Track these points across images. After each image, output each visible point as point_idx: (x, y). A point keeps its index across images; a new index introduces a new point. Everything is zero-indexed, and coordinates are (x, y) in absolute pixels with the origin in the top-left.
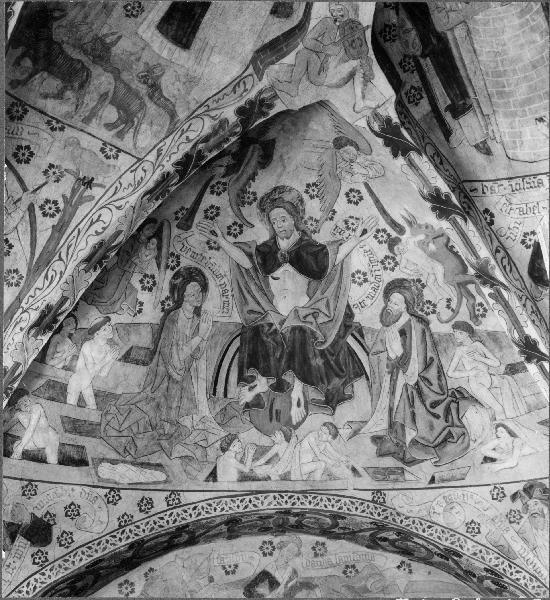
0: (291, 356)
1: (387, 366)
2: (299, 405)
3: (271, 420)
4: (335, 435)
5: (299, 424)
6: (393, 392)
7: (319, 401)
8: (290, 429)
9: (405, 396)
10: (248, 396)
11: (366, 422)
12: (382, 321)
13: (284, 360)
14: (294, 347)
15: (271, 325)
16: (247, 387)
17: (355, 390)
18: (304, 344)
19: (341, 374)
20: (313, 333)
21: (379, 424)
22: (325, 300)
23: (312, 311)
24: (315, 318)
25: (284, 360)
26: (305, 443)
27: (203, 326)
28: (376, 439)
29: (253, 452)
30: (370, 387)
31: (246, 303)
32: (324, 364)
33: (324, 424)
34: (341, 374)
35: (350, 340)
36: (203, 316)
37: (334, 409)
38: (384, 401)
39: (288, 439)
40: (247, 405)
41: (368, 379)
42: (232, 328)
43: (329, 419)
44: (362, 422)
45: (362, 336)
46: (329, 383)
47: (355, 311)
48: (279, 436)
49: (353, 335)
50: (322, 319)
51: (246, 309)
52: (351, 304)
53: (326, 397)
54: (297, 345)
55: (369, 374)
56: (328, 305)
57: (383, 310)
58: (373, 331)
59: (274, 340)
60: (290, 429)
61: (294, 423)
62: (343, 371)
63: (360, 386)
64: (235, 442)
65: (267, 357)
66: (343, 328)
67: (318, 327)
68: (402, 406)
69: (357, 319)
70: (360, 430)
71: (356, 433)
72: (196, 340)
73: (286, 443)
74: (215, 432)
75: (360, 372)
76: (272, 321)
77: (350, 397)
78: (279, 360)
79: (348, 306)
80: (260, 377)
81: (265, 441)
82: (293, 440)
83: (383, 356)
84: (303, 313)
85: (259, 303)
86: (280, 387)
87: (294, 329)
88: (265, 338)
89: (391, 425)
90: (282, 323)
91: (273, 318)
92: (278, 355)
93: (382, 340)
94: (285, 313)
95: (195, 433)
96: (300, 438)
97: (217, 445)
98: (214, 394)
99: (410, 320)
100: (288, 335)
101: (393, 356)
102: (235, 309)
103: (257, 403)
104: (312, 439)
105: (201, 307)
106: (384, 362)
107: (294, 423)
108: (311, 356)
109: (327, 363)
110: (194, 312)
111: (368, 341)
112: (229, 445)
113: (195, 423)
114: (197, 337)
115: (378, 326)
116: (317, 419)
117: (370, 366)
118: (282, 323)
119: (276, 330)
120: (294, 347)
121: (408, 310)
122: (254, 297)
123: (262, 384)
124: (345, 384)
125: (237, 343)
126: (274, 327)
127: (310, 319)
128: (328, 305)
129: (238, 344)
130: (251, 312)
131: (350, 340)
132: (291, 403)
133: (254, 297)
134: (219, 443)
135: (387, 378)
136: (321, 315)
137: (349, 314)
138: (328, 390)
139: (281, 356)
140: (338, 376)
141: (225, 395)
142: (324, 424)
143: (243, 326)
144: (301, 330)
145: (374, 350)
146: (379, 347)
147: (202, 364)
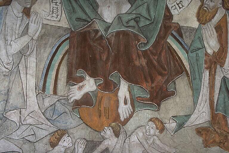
0: (116, 59)
1: (206, 62)
2: (126, 103)
3: (100, 116)
4: (162, 129)
5: (127, 120)
6: (212, 86)
7: (143, 99)
8: (119, 126)
9: (224, 89)
10: (77, 94)
11: (190, 115)
12: (199, 20)
13: (109, 63)
14: (118, 51)
15: (97, 31)
16: (76, 87)
17: (177, 87)
18: (127, 46)
19: (164, 72)
20: (136, 36)
21: (201, 115)
22: (146, 5)
23: (134, 16)
24: (137, 22)
25: (109, 63)
26: (134, 138)
27: (33, 27)
28: (200, 131)
29: (83, 147)
30: (190, 83)
31: (74, 11)
32: (147, 64)
33: (151, 120)
34: (164, 72)
35: (170, 41)
36: (33, 17)
37: (159, 105)
38: (205, 91)
39: (117, 135)
40: (78, 104)
41: (188, 77)
42: (61, 32)
43: (156, 115)
44: (186, 116)
45: (181, 36)
46: (152, 82)
47: (174, 12)
48: (108, 132)
49: (172, 35)
50: (141, 24)
51: (74, 17)
52: (170, 6)
53: (151, 93)
54: (122, 48)
55: (188, 68)
56: (148, 10)
57: (200, 8)
58: (192, 30)
59: (100, 45)
60: (119, 126)
61: (122, 119)
62: (165, 70)
63: (182, 84)
64: (65, 137)
65: (94, 60)
66: (163, 29)
67: (140, 29)
68: (221, 99)
69: (175, 19)
70: (184, 123)
71: (180, 126)
72: (25, 40)
73: (116, 139)
74: (43, 126)
75: (180, 70)
76: (97, 28)
77: (173, 94)
78: (106, 63)
79: (167, 9)
80: (88, 78)
81: (95, 137)
82: (121, 136)
83: (201, 53)
84: (125, 19)
85: (86, 14)
86: (109, 87)
87: (118, 33)
88: (92, 43)
89: (214, 116)
90: (107, 29)
91: (99, 26)
92: (104, 58)
93: (199, 37)
94: (109, 21)
95: (24, 128)
96: (129, 134)
97: (46, 140)
98: (44, 89)
99: (225, 15)
100: (113, 40)
101: (210, 51)
102: (64, 15)
103: (86, 100)
104: (141, 134)
105: (30, 8)
106: (202, 59)
107: (122, 119)
108: (134, 57)
109: (150, 63)
110: (24, 12)
111: (187, 41)
112: (59, 140)
113: (23, 119)
114: (26, 36)
115: (195, 24)
116: (145, 115)
117: (190, 64)
118: (107, 29)
119: (102, 36)
120: (118, 51)
121: (223, 6)
122: (81, 7)
123: (90, 85)
124: (167, 82)
125: (65, 47)
126: (100, 34)
127: (132, 23)
128: (148, 10)
129: (67, 47)
130: (78, 19)
131: (170, 41)
132: (118, 101)
133: (81, 7)
134: (48, 138)
135: (207, 73)
136: (142, 19)
137: (169, 16)
138: (152, 88)
139: (108, 59)
140: (161, 74)
141: (55, 92)
142: (151, 120)
143: (72, 32)
144: (125, 33)
145: (192, 48)
146: (198, 45)
147: (32, 61)
